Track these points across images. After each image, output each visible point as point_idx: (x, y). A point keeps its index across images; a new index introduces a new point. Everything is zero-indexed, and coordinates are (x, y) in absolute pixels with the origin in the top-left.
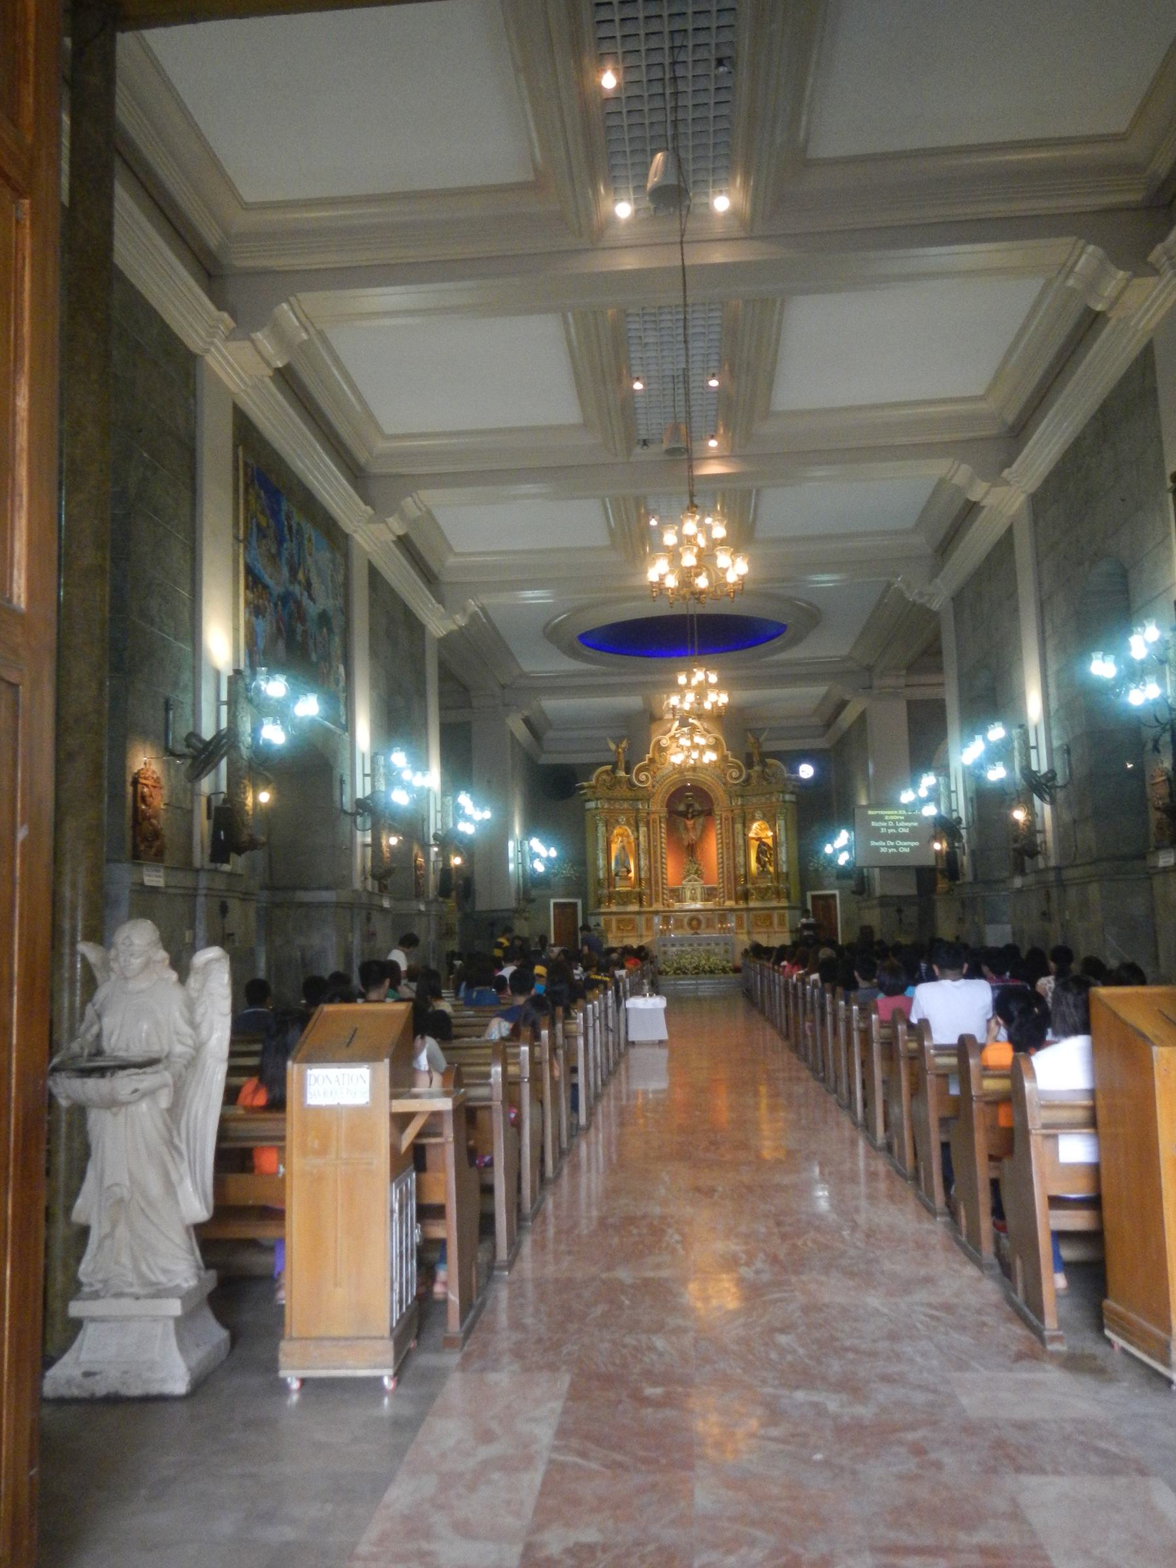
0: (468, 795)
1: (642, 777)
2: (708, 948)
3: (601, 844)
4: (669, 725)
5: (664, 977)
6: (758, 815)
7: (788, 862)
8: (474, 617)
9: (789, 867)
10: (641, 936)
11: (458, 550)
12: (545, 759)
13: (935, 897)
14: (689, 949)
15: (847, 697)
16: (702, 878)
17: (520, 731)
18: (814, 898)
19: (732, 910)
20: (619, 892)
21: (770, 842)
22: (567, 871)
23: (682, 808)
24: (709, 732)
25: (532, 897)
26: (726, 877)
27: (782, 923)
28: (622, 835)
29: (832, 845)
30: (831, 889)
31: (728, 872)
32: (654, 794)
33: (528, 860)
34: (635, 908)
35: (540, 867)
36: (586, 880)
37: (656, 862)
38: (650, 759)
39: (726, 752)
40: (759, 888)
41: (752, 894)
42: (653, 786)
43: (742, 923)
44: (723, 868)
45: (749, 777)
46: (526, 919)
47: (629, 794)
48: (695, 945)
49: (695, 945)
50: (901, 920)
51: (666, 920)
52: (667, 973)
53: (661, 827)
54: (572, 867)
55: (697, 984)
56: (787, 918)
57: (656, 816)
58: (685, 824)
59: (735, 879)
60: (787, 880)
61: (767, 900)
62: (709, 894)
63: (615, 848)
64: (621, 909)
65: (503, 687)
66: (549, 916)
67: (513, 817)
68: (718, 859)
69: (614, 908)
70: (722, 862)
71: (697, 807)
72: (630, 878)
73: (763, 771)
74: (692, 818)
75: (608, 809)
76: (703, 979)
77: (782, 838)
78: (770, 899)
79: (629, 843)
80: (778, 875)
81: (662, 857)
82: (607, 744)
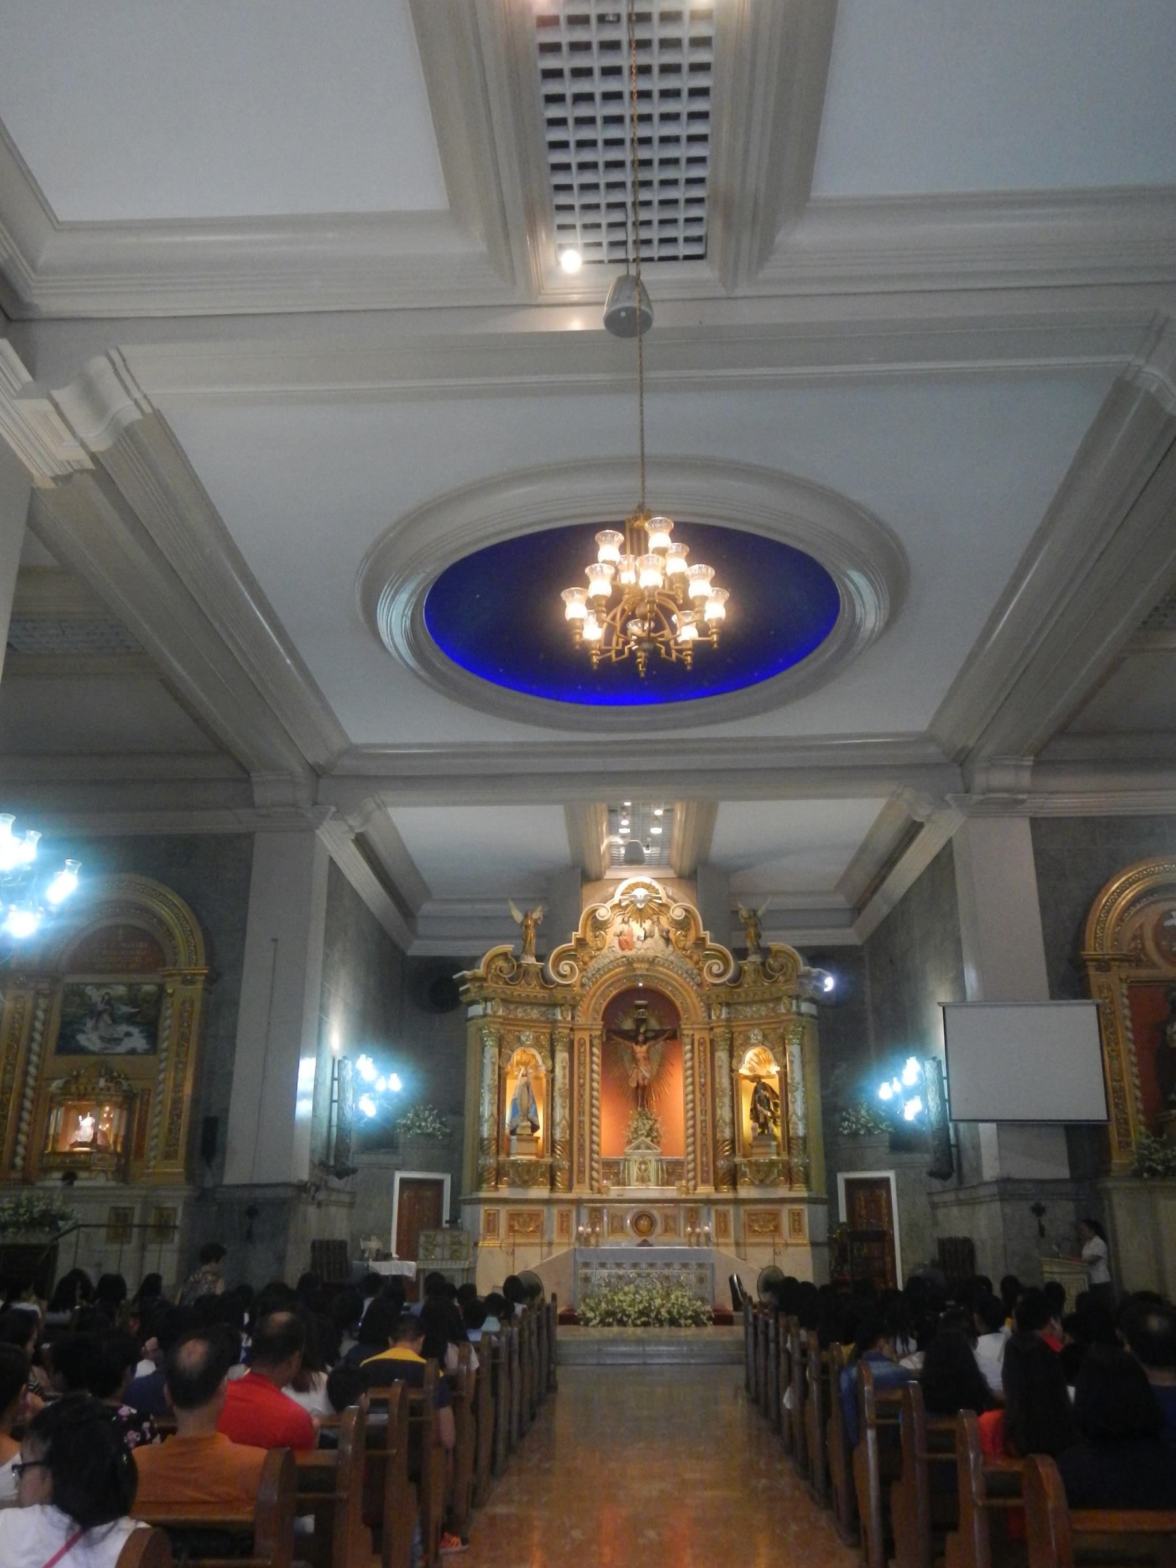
0: (34, 836)
1: (564, 968)
2: (666, 1272)
3: (489, 1077)
4: (611, 889)
5: (582, 1329)
6: (755, 1035)
7: (806, 1116)
8: (127, 435)
9: (806, 1126)
10: (550, 1244)
11: (65, 211)
12: (417, 949)
13: (1110, 1184)
14: (632, 1273)
15: (918, 819)
16: (658, 1143)
17: (359, 874)
18: (850, 1183)
19: (709, 1202)
20: (514, 1163)
21: (775, 1084)
22: (430, 1124)
23: (628, 1025)
24: (675, 901)
25: (349, 1164)
26: (698, 1143)
27: (797, 1228)
28: (526, 1064)
29: (900, 1080)
30: (878, 1169)
31: (704, 1135)
32: (582, 996)
33: (350, 1095)
34: (540, 1192)
35: (369, 1109)
36: (462, 1140)
37: (581, 1113)
38: (578, 940)
39: (702, 932)
40: (757, 1164)
41: (744, 1174)
42: (583, 985)
43: (726, 1224)
44: (694, 1126)
45: (740, 973)
46: (319, 1205)
47: (542, 994)
48: (644, 1266)
49: (644, 1266)
50: (1042, 1230)
51: (595, 1216)
52: (587, 1322)
53: (592, 1054)
54: (439, 1116)
55: (644, 1355)
56: (806, 1220)
57: (586, 1036)
58: (633, 1053)
59: (715, 1148)
60: (805, 1149)
61: (767, 1186)
62: (671, 1172)
63: (513, 1087)
64: (518, 1194)
65: (317, 772)
66: (391, 1202)
67: (323, 1009)
68: (687, 1112)
69: (505, 1192)
70: (694, 1117)
71: (654, 1024)
72: (538, 1138)
73: (763, 964)
74: (644, 1043)
75: (505, 1018)
76: (659, 1342)
77: (796, 1075)
78: (774, 1184)
79: (537, 1078)
80: (788, 1140)
81: (592, 1106)
82: (510, 911)
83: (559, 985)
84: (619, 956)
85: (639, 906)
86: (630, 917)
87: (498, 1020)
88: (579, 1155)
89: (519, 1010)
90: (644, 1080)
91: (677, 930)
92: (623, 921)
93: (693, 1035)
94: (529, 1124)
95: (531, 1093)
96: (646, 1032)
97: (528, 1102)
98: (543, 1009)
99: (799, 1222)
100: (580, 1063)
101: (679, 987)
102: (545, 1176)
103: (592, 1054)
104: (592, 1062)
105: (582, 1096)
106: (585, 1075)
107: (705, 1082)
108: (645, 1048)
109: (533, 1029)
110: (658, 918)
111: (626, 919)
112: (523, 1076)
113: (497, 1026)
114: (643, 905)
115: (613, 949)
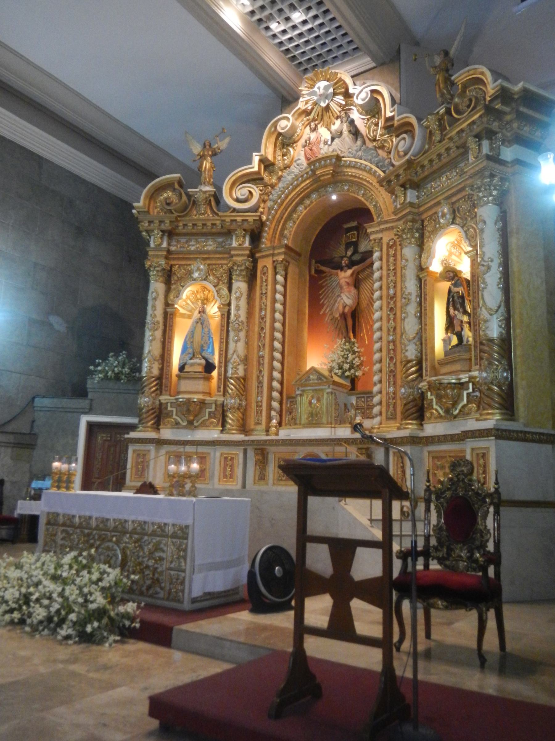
1: (241, 192)
53: (275, 282)
66: (76, 444)
69: (167, 433)
74: (349, 267)
78: (464, 413)
83: (234, 210)
84: (304, 168)
85: (323, 105)
86: (319, 123)
87: (160, 253)
88: (258, 393)
89: (192, 243)
90: (344, 307)
91: (368, 120)
92: (311, 128)
93: (382, 238)
94: (203, 362)
95: (206, 330)
96: (353, 254)
97: (202, 340)
98: (220, 240)
99: (485, 466)
100: (262, 294)
101: (370, 186)
102: (215, 418)
103: (275, 282)
104: (275, 291)
105: (262, 329)
106: (266, 306)
107: (395, 294)
108: (349, 272)
109: (209, 262)
110: (346, 113)
111: (313, 125)
112: (200, 312)
113: (159, 260)
114: (327, 102)
115: (298, 162)
